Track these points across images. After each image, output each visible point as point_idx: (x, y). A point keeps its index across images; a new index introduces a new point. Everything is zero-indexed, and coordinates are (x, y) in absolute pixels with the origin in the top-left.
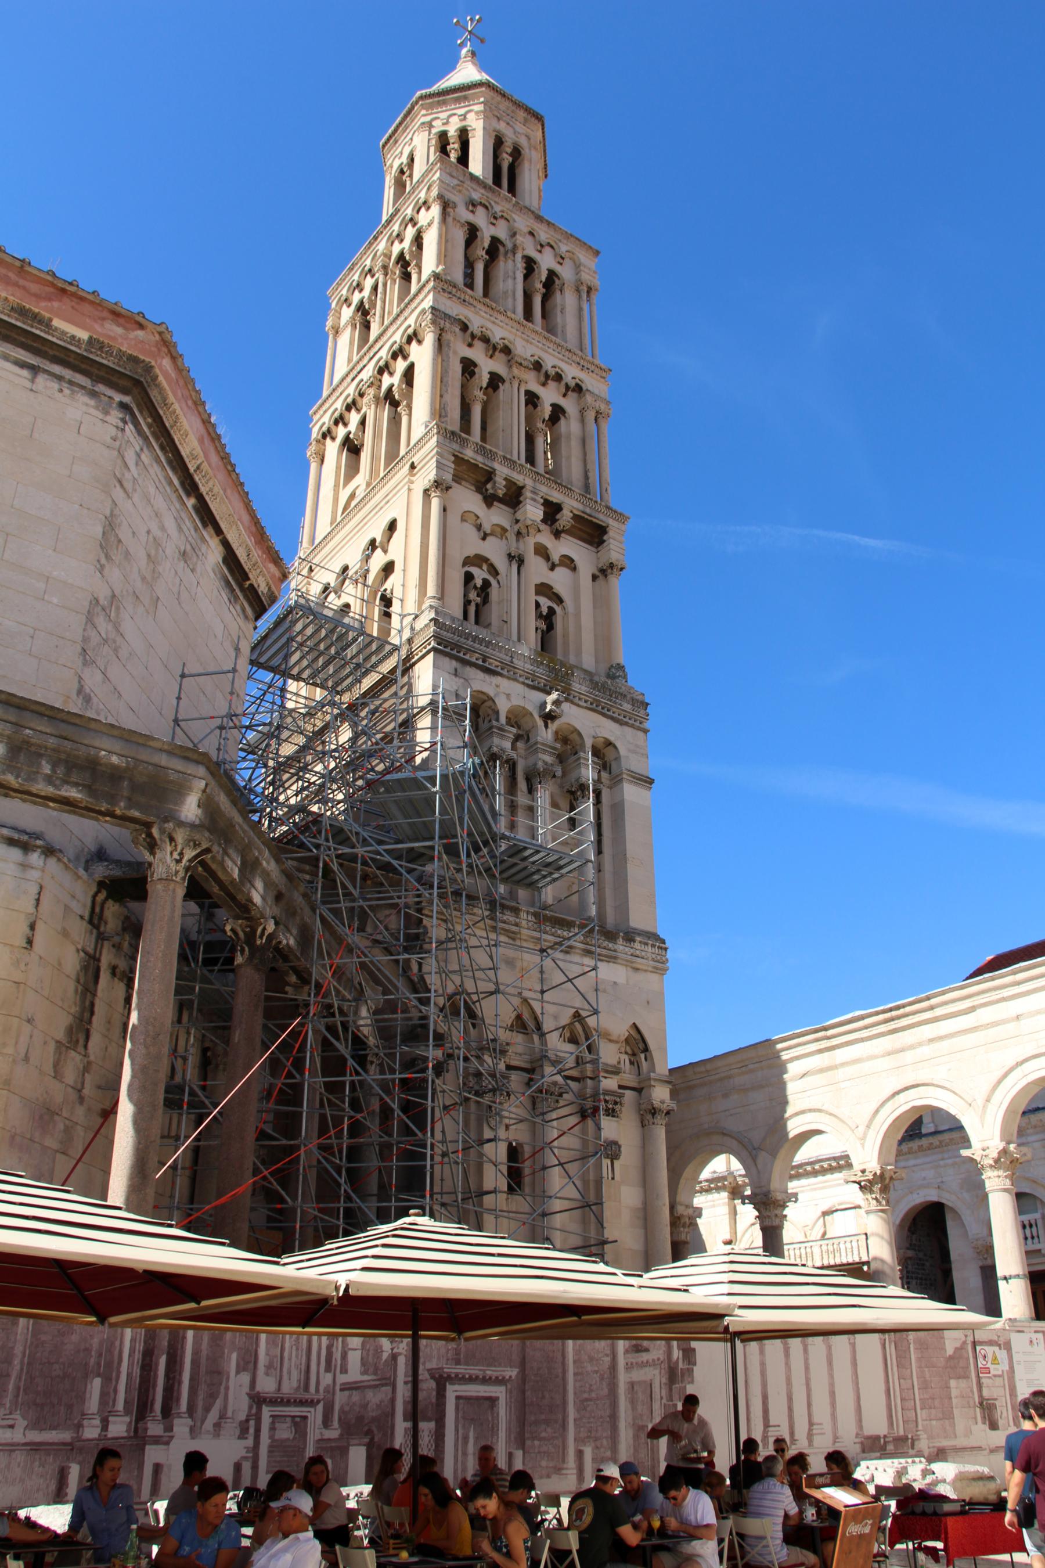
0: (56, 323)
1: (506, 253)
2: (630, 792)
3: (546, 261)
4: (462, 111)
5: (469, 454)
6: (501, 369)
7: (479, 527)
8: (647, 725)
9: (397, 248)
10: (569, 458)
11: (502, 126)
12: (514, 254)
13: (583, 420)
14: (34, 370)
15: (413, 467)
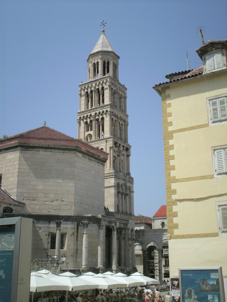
0: (101, 157)
1: (116, 93)
2: (132, 193)
3: (120, 93)
4: (108, 57)
5: (115, 141)
6: (116, 120)
7: (114, 151)
8: (134, 183)
9: (97, 87)
10: (123, 133)
11: (114, 61)
12: (117, 93)
13: (125, 126)
14: (98, 163)
15: (106, 141)
